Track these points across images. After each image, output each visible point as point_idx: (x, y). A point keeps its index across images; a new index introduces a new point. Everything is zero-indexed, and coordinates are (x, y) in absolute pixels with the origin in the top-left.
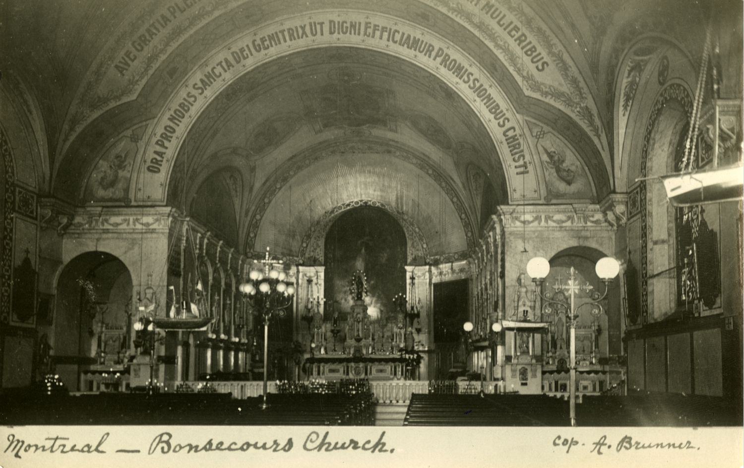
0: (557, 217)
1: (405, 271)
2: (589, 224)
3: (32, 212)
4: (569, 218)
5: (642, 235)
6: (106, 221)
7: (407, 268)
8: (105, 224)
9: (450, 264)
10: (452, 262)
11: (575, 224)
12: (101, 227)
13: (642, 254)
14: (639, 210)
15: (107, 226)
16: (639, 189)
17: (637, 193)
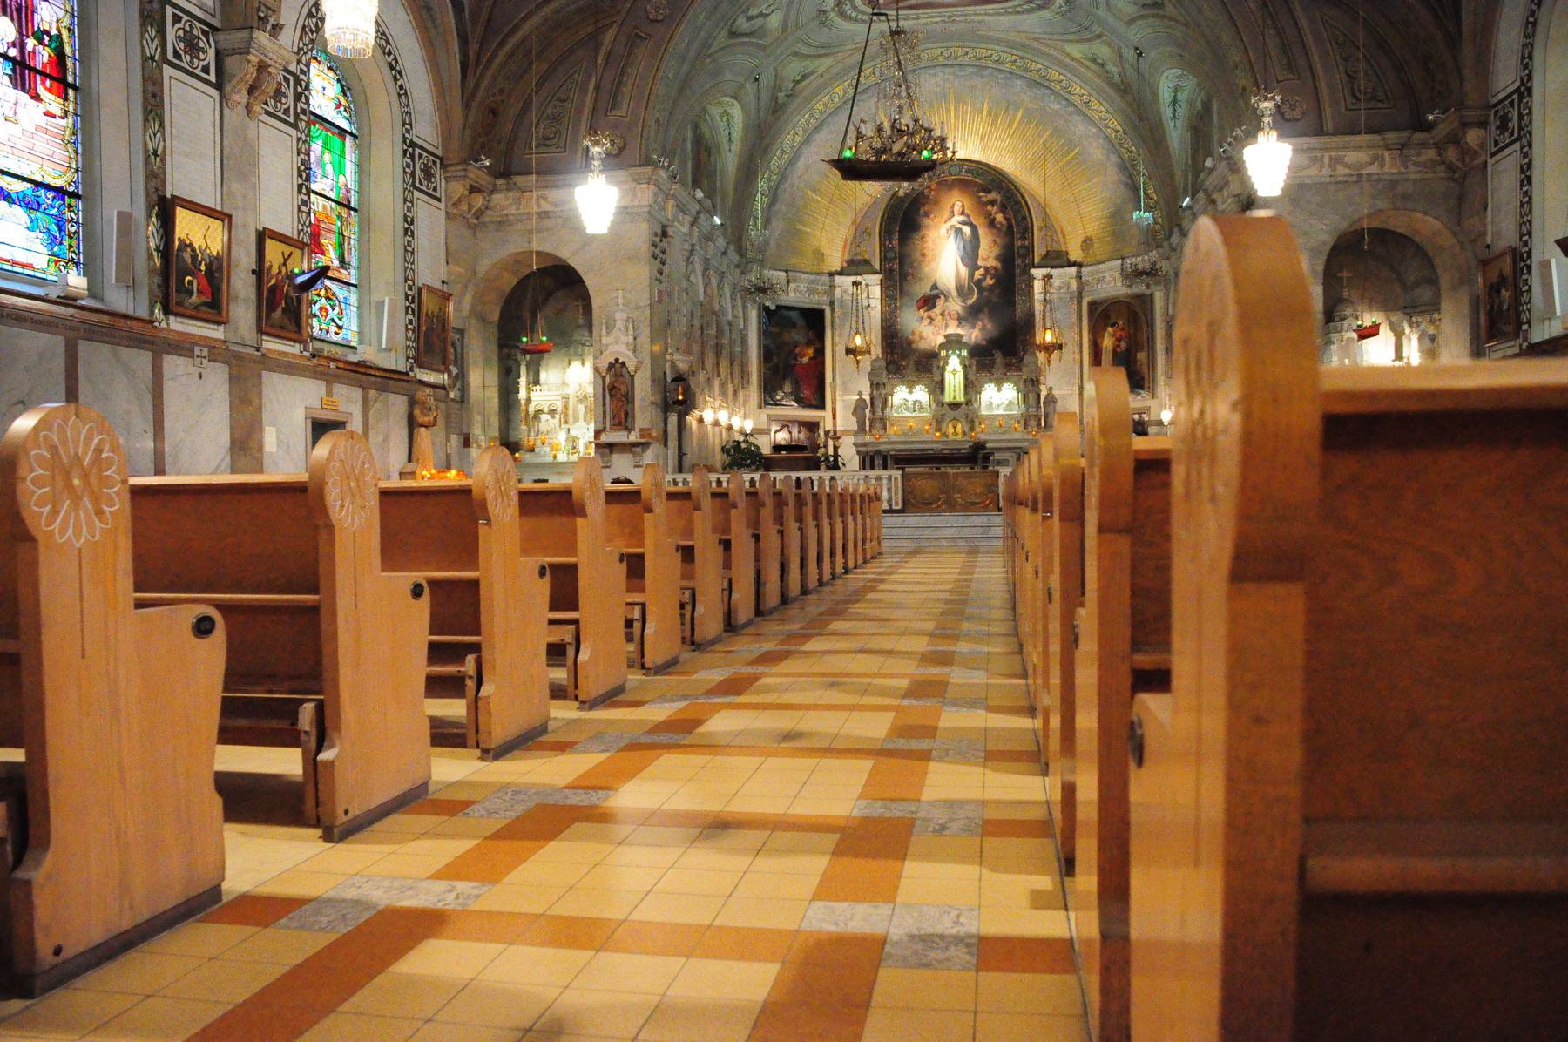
0: (1353, 157)
1: (1030, 280)
2: (1412, 168)
3: (435, 189)
4: (1375, 159)
5: (1522, 182)
6: (545, 198)
7: (1038, 273)
8: (542, 202)
9: (1120, 262)
10: (1123, 259)
11: (1386, 169)
12: (535, 209)
13: (1522, 217)
14: (1516, 135)
15: (545, 206)
16: (1516, 96)
17: (1512, 104)
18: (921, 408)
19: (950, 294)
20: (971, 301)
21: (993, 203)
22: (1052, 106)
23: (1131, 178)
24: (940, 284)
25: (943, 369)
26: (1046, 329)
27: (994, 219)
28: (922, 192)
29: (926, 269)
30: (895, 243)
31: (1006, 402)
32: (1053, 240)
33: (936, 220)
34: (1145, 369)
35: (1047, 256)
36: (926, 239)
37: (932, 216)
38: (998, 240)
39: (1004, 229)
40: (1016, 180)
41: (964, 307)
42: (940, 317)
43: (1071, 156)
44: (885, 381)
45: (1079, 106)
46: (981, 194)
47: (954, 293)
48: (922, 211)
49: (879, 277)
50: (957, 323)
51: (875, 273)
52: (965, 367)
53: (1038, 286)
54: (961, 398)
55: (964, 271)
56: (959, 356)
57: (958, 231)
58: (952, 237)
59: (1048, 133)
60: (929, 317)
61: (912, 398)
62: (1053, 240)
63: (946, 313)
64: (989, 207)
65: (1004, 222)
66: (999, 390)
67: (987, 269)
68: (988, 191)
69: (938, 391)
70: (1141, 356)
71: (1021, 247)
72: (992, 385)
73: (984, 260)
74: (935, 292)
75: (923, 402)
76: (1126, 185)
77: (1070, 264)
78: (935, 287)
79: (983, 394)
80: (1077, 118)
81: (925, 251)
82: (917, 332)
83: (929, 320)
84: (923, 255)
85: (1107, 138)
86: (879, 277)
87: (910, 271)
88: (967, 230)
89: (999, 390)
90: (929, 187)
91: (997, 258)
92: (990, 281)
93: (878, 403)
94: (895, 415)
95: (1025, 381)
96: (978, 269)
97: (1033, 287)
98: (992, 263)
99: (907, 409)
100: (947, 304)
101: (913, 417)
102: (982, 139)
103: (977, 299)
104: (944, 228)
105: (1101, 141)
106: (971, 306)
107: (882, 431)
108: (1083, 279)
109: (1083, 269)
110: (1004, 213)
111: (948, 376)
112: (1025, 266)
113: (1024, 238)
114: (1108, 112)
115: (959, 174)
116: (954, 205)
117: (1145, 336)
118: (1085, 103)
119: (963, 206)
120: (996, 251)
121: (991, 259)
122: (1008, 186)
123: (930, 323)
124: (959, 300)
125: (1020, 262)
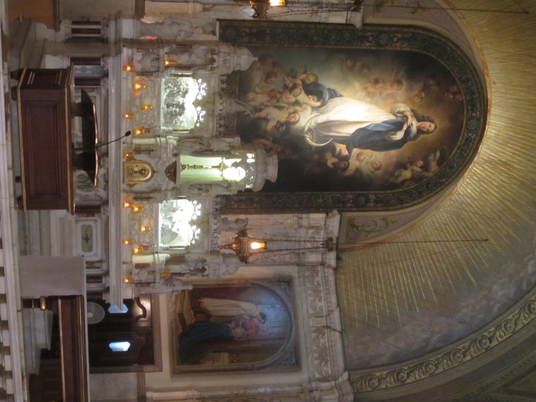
1: (326, 209)
7: (335, 220)
9: (338, 327)
10: (341, 333)
18: (172, 116)
19: (321, 113)
20: (309, 139)
21: (426, 167)
22: (532, 262)
23: (435, 350)
24: (336, 100)
25: (227, 154)
26: (266, 243)
27: (406, 168)
28: (454, 82)
29: (357, 85)
30: (398, 46)
31: (174, 230)
32: (369, 232)
33: (417, 100)
34: (208, 365)
35: (352, 225)
36: (396, 87)
37: (423, 95)
38: (379, 172)
39: (392, 180)
40: (448, 191)
41: (303, 129)
42: (293, 99)
43: (469, 273)
44: (216, 70)
45: (526, 297)
46: (438, 154)
47: (322, 119)
48: (431, 82)
49: (358, 25)
50: (283, 120)
51: (363, 19)
52: (228, 184)
53: (318, 218)
54: (184, 174)
55: (349, 131)
56: (246, 180)
57: (397, 126)
58: (393, 118)
59: (499, 249)
60: (295, 86)
61: (188, 101)
62: (369, 232)
63: (298, 108)
64: (421, 163)
65: (400, 179)
66: (192, 223)
67: (346, 159)
68: (439, 163)
69: (197, 147)
70: (224, 359)
71: (367, 197)
72: (199, 213)
73: (358, 156)
74: (327, 97)
75: (181, 118)
76: (427, 342)
77: (338, 259)
78: (334, 94)
79: (187, 201)
80: (512, 291)
81: (381, 85)
82: (276, 70)
83: (291, 85)
84: (376, 82)
85: (484, 325)
86: (358, 25)
87: (358, 64)
88: (399, 136)
89: (192, 223)
90: (459, 93)
91: (358, 170)
92: (331, 161)
93: (184, 59)
94: (163, 80)
95: (204, 261)
96: (349, 149)
97: (317, 211)
98: (354, 164)
99: (172, 95)
100: (309, 109)
101: (159, 106)
102: (505, 164)
103: (310, 147)
104: (403, 107)
105: (481, 316)
106: (303, 138)
107: (139, 67)
108: (320, 268)
109: (331, 271)
110: (412, 179)
111: (217, 160)
112: (344, 203)
113: (377, 202)
114: (514, 333)
115: (466, 127)
116: (432, 121)
117: (249, 364)
118: (529, 306)
119: (428, 132)
120: (366, 169)
121: (357, 163)
122: (441, 184)
123: (286, 87)
124: (313, 124)
125: (350, 197)
